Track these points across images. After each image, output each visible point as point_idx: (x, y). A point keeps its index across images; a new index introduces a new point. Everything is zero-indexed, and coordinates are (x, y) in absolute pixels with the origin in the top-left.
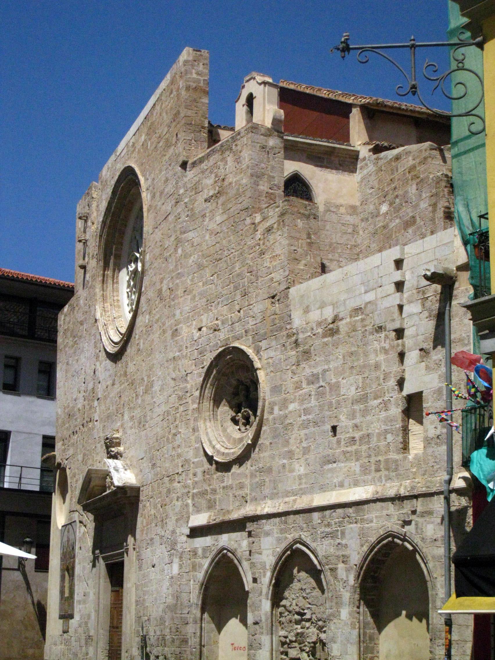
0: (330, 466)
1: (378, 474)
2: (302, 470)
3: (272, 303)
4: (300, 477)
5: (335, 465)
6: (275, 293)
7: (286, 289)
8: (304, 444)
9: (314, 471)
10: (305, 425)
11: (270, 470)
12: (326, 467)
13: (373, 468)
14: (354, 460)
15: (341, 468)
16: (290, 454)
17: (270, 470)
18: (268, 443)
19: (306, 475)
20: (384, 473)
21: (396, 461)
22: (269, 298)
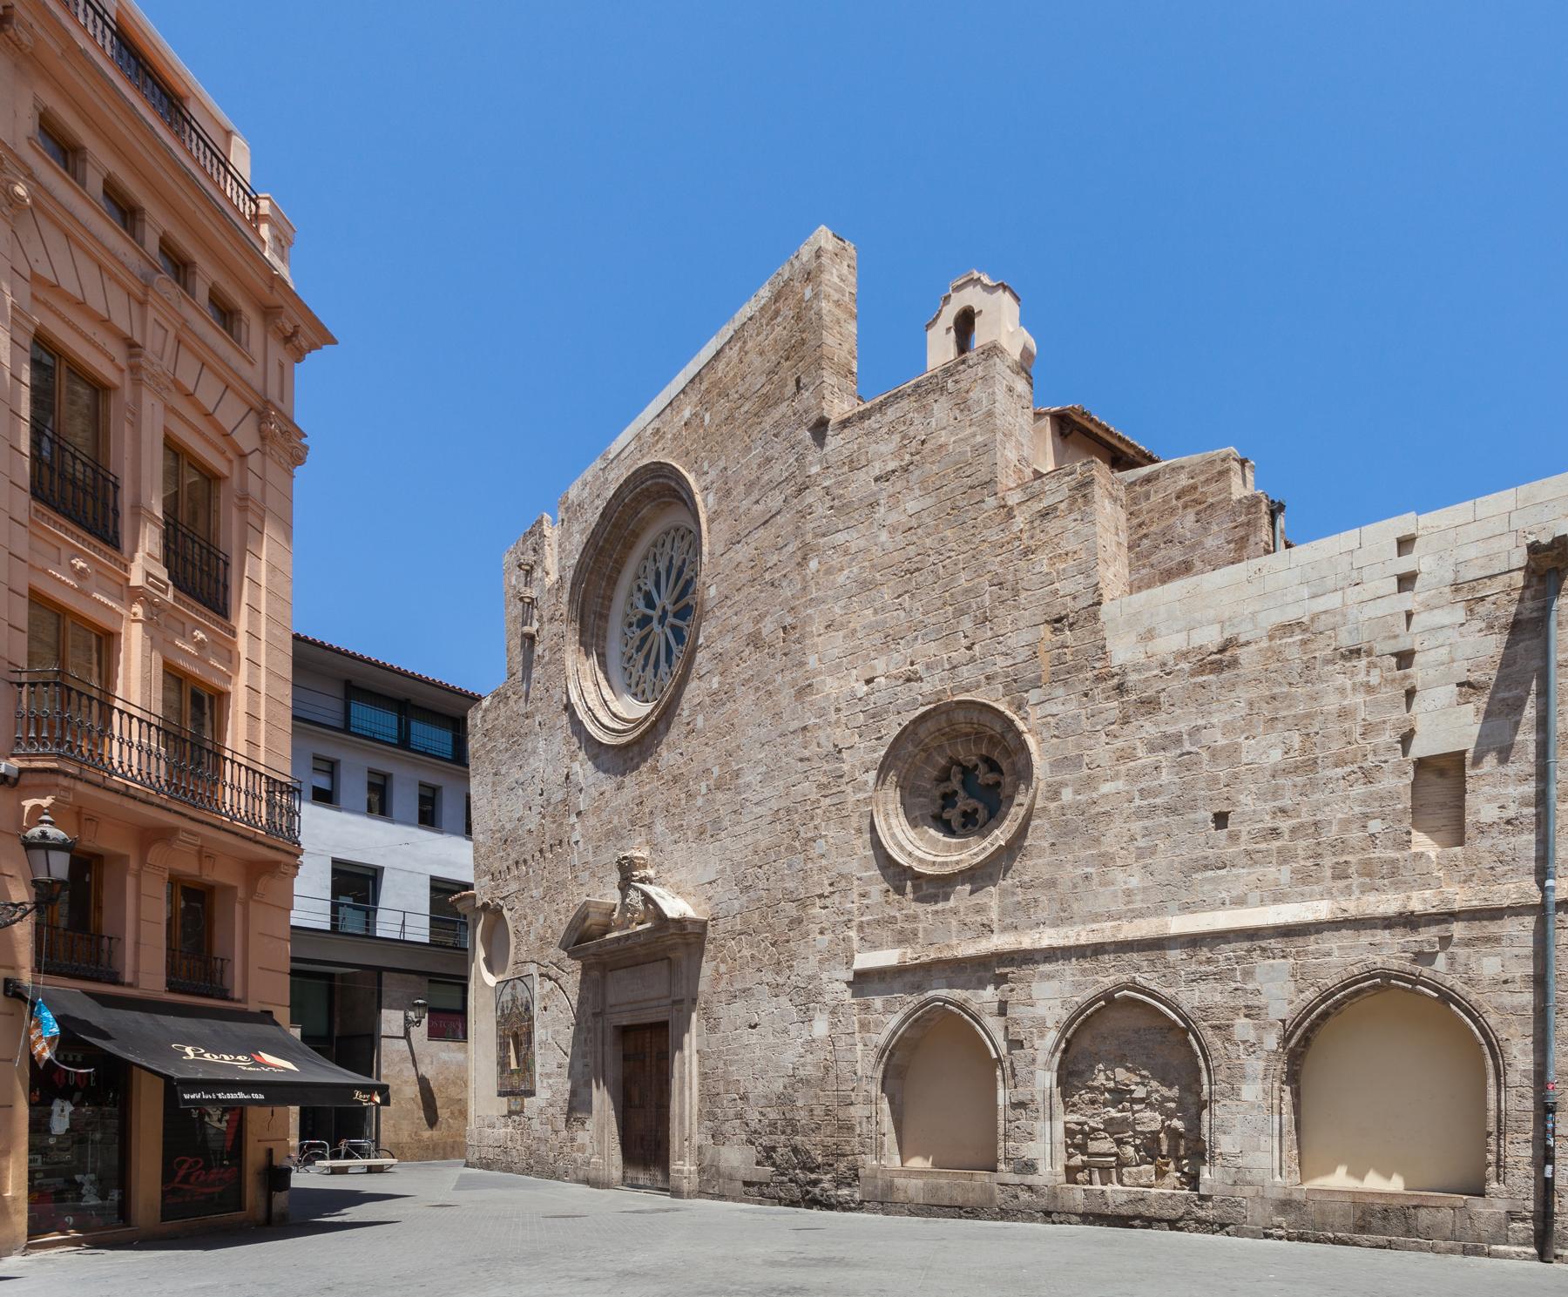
0: (1210, 874)
1: (1342, 884)
2: (1134, 882)
3: (1056, 629)
4: (1129, 893)
5: (1223, 872)
6: (1063, 613)
7: (1090, 606)
8: (1141, 843)
9: (1167, 882)
10: (1139, 814)
11: (1052, 883)
12: (1198, 876)
13: (1328, 873)
14: (1274, 862)
15: (1237, 876)
16: (1105, 860)
17: (1052, 883)
18: (1046, 844)
19: (1145, 889)
20: (1356, 881)
21: (1394, 861)
22: (1047, 622)
